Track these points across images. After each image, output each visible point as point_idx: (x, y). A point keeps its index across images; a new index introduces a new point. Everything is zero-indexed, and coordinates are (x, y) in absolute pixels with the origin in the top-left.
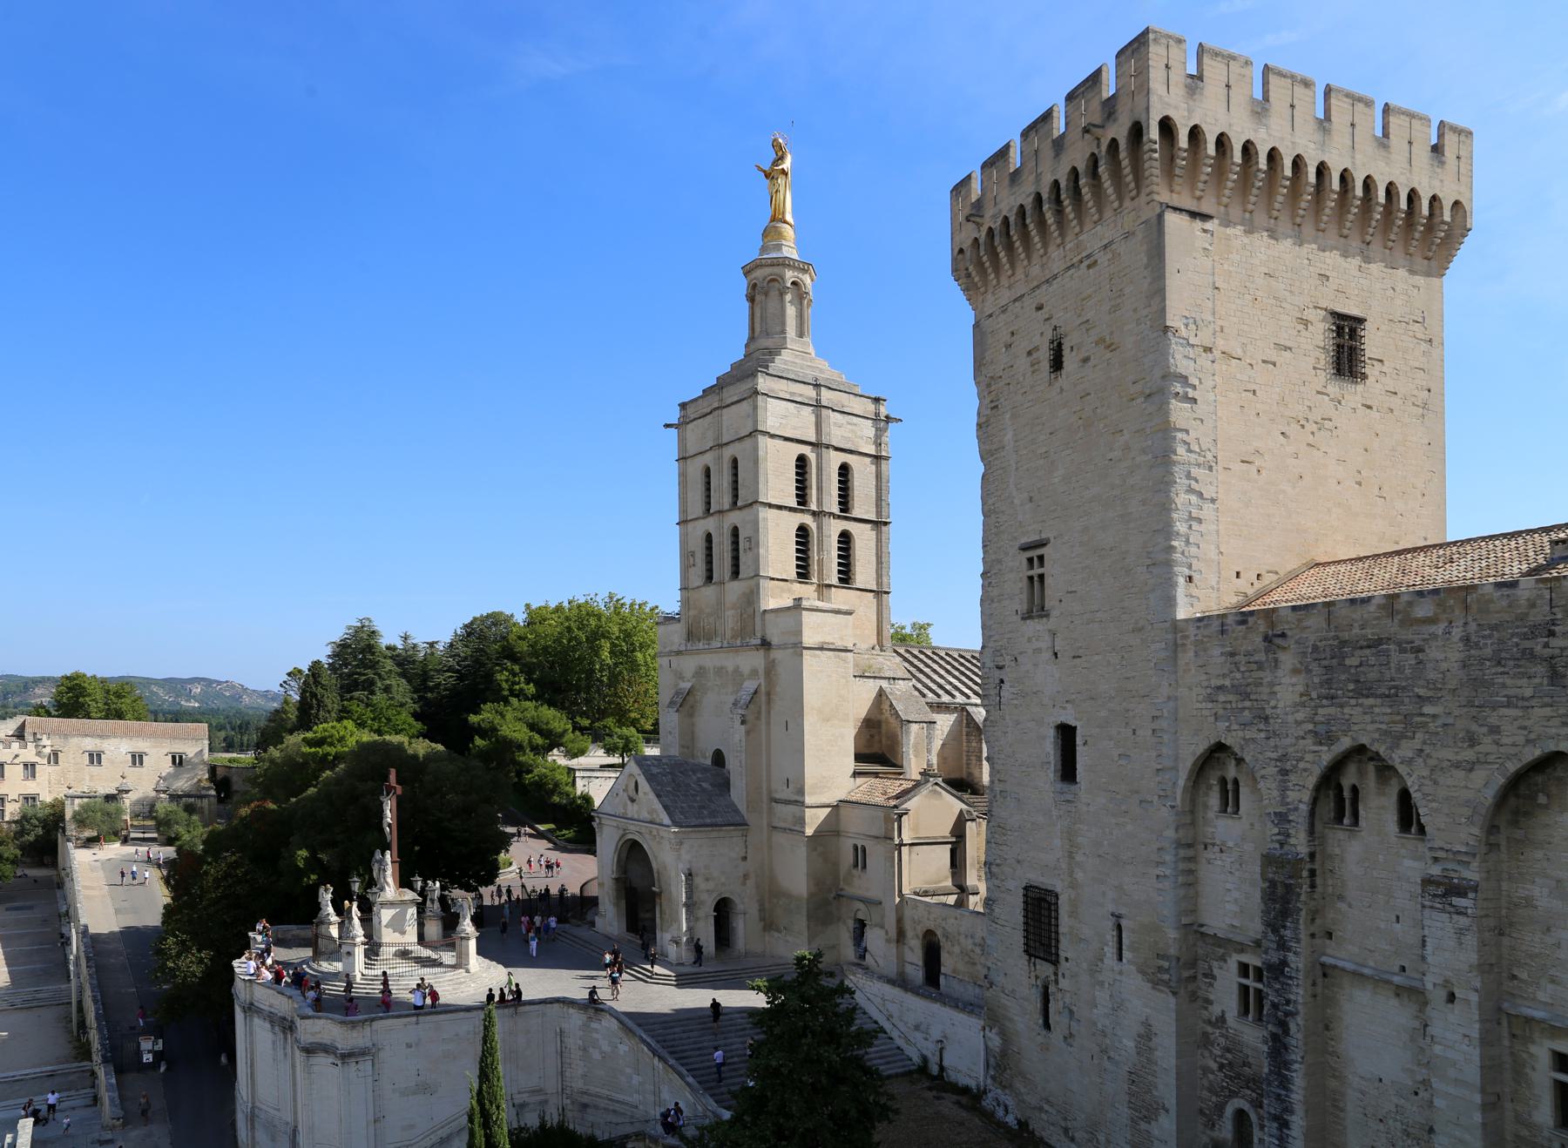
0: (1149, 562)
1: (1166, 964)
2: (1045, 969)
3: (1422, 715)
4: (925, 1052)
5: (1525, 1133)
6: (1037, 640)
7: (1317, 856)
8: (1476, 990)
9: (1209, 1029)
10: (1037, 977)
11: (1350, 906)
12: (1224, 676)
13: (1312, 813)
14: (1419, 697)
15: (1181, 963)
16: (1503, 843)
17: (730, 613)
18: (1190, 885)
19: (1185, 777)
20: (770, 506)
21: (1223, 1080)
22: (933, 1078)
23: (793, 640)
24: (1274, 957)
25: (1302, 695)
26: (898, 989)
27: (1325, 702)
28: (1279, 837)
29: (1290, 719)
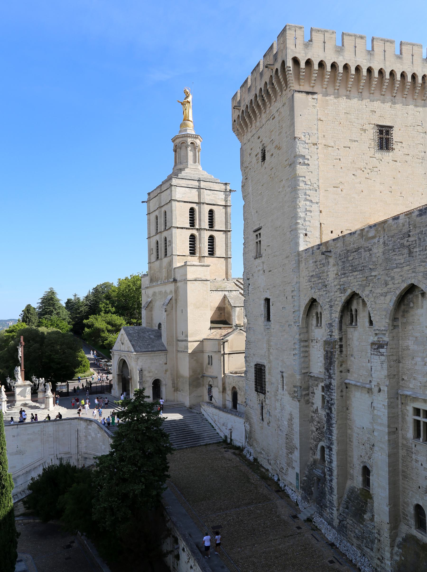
0: (290, 230)
1: (296, 389)
2: (262, 396)
3: (371, 276)
4: (226, 434)
5: (405, 442)
6: (259, 266)
7: (344, 339)
8: (387, 386)
9: (313, 415)
10: (260, 400)
11: (355, 358)
12: (313, 271)
13: (341, 322)
14: (370, 269)
15: (302, 389)
16: (400, 325)
17: (164, 270)
18: (306, 357)
19: (302, 314)
20: (178, 228)
21: (317, 435)
22: (229, 444)
23: (184, 278)
25: (336, 274)
26: (217, 410)
27: (343, 276)
28: (330, 333)
29: (333, 285)
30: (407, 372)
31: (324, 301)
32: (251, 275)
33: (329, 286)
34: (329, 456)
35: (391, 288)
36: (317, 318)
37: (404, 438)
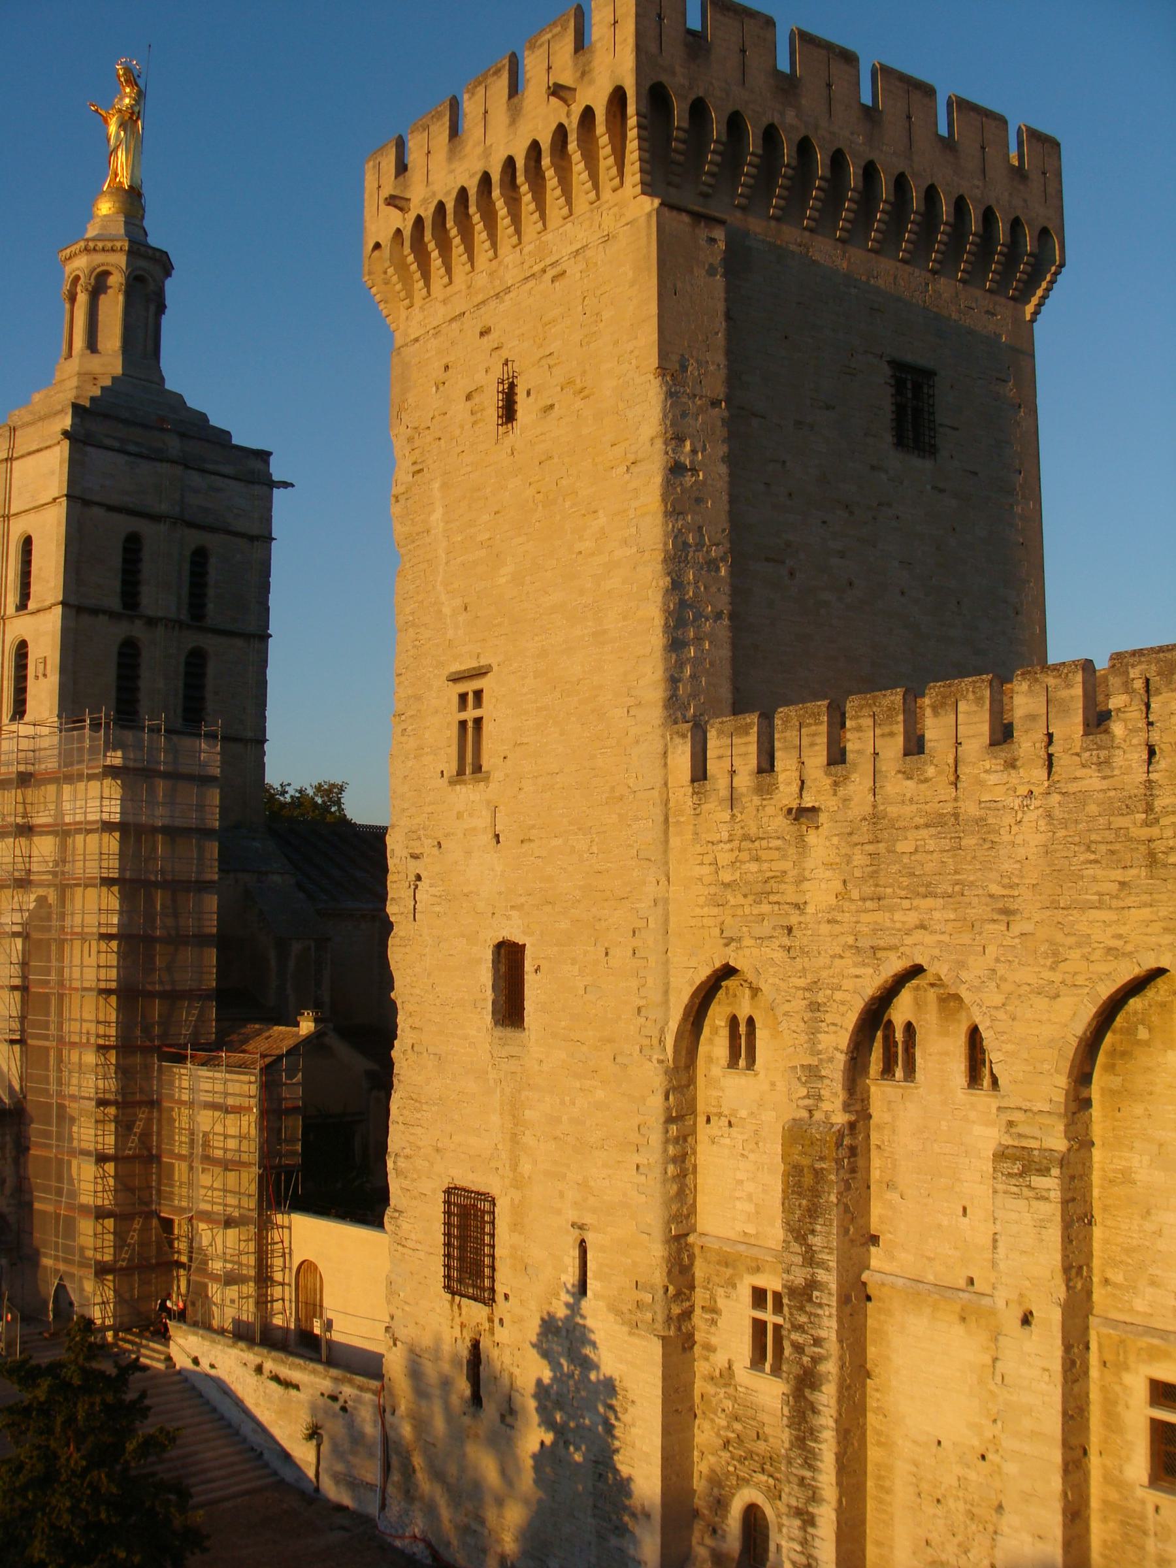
0: (631, 701)
2: (475, 1312)
10: (462, 1326)
24: (799, 1277)
27: (869, 904)
30: (1125, 1258)
31: (783, 985)
32: (428, 842)
33: (810, 932)
34: (802, 1544)
35: (1075, 974)
37: (1113, 1480)
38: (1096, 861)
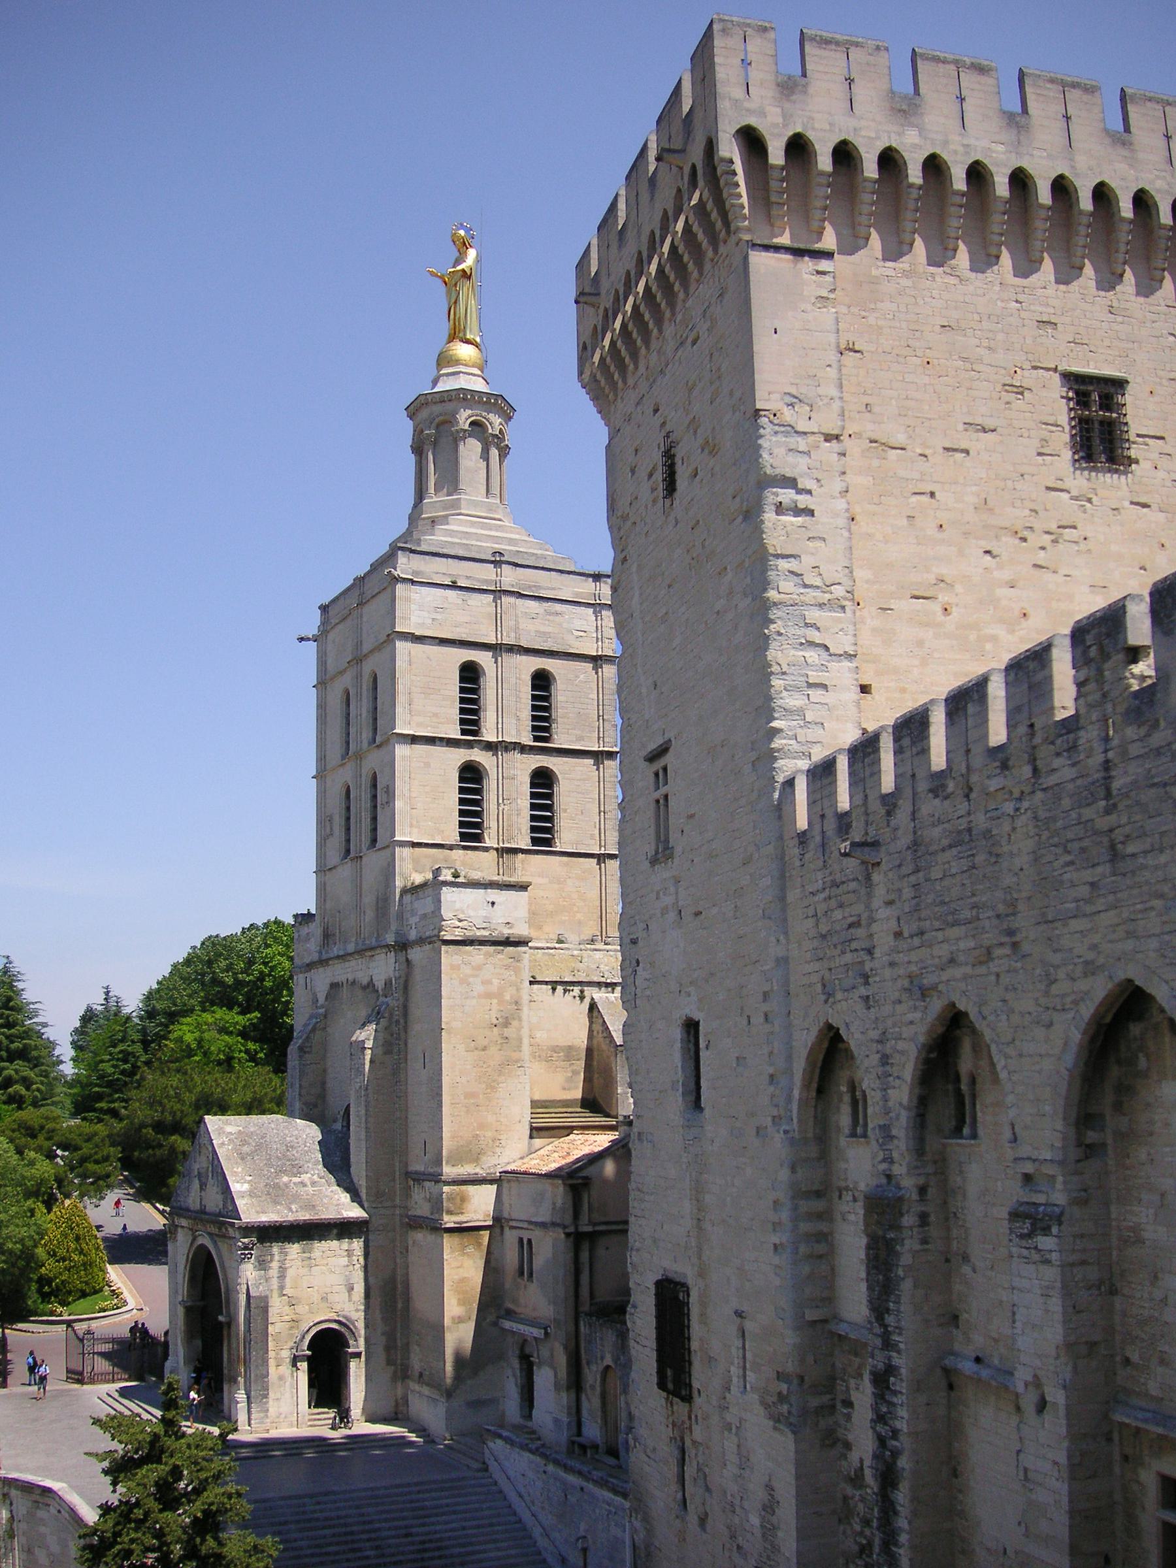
2: (681, 1408)
7: (932, 1192)
9: (849, 1491)
10: (674, 1424)
16: (1110, 1141)
28: (884, 1166)
32: (642, 926)
33: (877, 979)
36: (855, 1103)
38: (1072, 863)
